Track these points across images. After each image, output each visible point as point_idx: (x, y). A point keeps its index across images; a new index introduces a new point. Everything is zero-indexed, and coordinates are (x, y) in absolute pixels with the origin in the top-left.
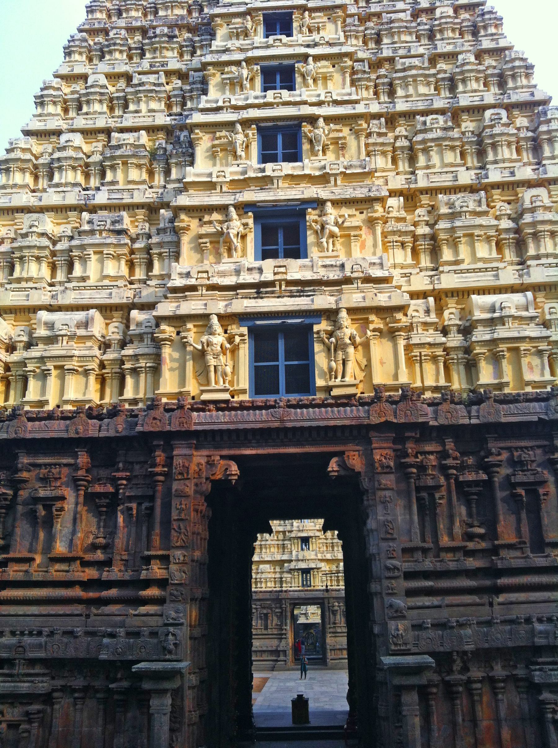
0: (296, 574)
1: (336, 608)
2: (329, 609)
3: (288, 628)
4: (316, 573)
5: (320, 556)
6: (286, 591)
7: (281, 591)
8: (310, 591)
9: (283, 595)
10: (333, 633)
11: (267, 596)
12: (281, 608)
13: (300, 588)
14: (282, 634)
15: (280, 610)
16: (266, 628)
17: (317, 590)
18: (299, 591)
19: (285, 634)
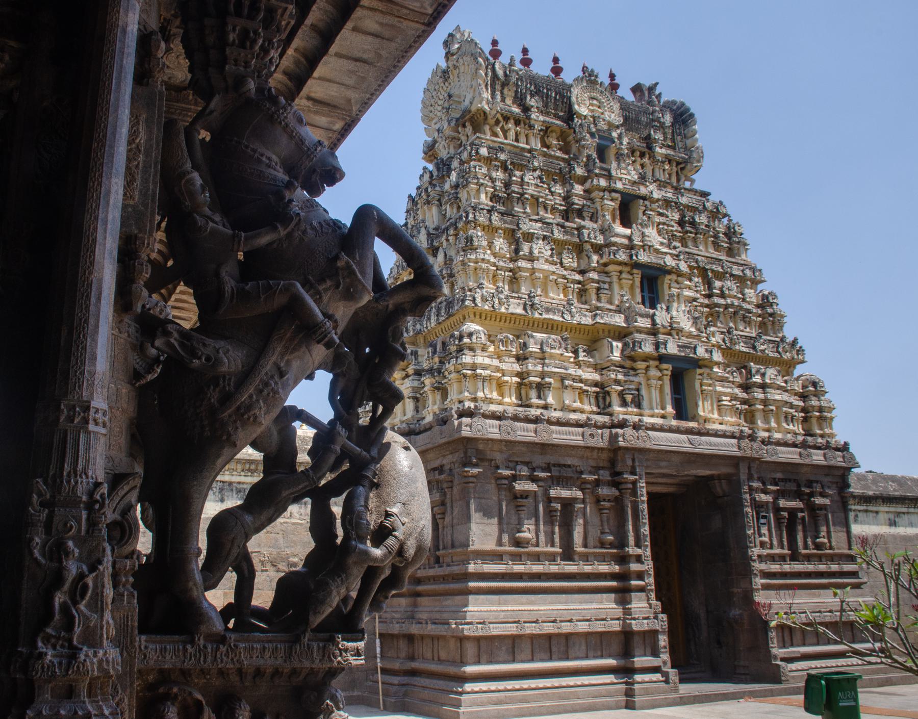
12: (616, 484)
15: (614, 492)
17: (716, 434)
19: (640, 576)
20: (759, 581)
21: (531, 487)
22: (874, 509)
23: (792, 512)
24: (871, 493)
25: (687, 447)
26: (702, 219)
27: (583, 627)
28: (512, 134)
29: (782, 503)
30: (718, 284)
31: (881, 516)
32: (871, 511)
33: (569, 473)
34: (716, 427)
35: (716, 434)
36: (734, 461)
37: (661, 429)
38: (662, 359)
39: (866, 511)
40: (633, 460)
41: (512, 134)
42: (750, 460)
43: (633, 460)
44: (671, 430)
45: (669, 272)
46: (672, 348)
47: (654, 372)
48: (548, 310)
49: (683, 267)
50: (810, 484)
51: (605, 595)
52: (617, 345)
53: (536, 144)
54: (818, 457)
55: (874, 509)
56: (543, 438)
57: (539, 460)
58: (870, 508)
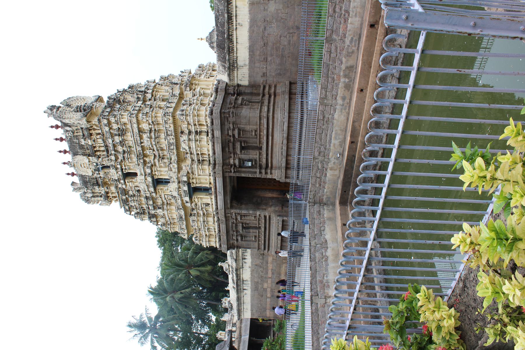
2: (238, 172)
8: (216, 189)
11: (223, 227)
13: (213, 197)
22: (234, 10)
23: (242, 148)
24: (226, 15)
29: (238, 152)
31: (238, 5)
32: (236, 11)
33: (234, 225)
39: (236, 15)
40: (228, 213)
43: (228, 213)
45: (153, 177)
46: (187, 199)
48: (181, 218)
51: (271, 222)
55: (234, 10)
57: (231, 232)
58: (234, 14)
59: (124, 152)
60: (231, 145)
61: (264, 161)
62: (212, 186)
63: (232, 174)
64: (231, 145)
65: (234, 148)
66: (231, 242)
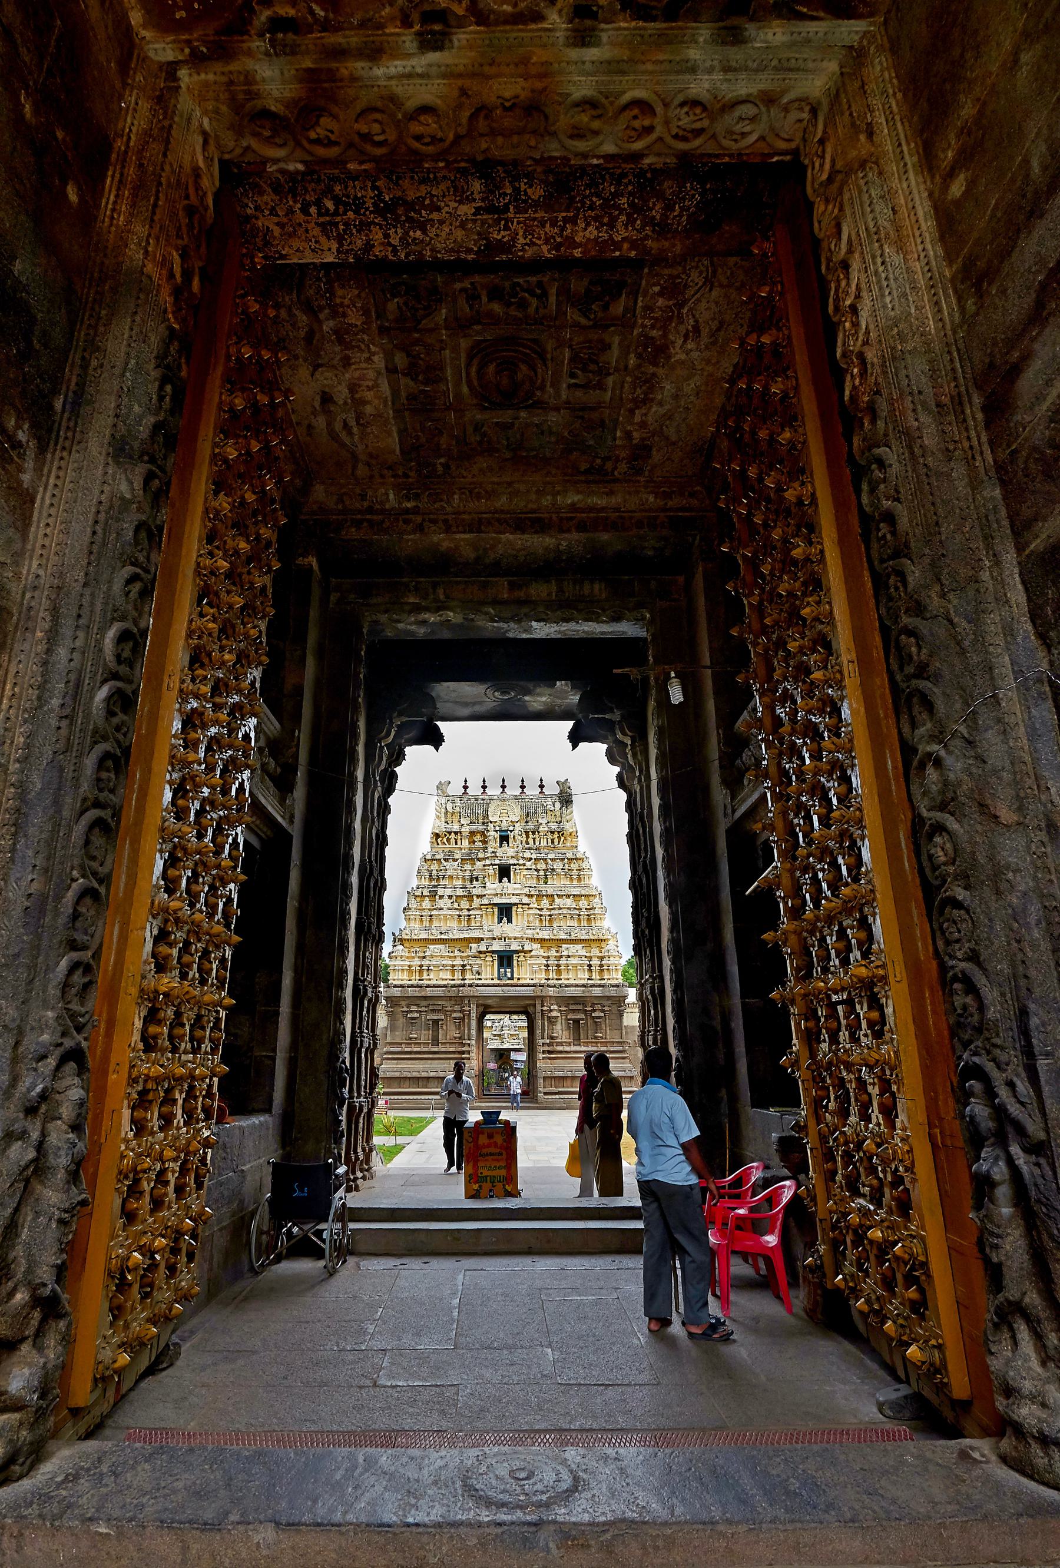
0: (489, 959)
1: (554, 1014)
3: (473, 1042)
4: (521, 959)
5: (530, 934)
6: (471, 986)
7: (464, 986)
9: (465, 991)
10: (549, 1052)
11: (440, 992)
13: (496, 981)
14: (463, 1053)
16: (435, 1041)
17: (523, 985)
18: (494, 985)
19: (468, 1052)
20: (541, 1056)
21: (416, 1015)
23: (577, 1022)
25: (501, 994)
26: (558, 865)
27: (432, 1074)
28: (453, 841)
30: (557, 900)
34: (528, 981)
35: (523, 985)
36: (533, 998)
37: (488, 986)
38: (493, 952)
41: (453, 841)
42: (542, 998)
44: (494, 985)
45: (516, 904)
46: (496, 946)
47: (489, 959)
49: (526, 900)
50: (593, 1005)
52: (473, 945)
53: (466, 843)
54: (597, 992)
56: (423, 994)
57: (424, 1003)
59: (537, 870)
60: (580, 1007)
61: (560, 1048)
62: (515, 981)
63: (538, 1008)
64: (580, 1007)
65: (573, 1011)
66: (403, 1003)
